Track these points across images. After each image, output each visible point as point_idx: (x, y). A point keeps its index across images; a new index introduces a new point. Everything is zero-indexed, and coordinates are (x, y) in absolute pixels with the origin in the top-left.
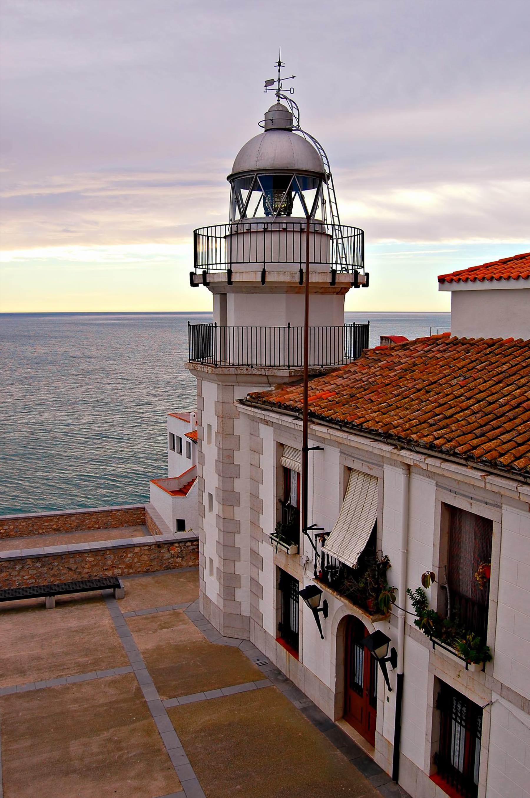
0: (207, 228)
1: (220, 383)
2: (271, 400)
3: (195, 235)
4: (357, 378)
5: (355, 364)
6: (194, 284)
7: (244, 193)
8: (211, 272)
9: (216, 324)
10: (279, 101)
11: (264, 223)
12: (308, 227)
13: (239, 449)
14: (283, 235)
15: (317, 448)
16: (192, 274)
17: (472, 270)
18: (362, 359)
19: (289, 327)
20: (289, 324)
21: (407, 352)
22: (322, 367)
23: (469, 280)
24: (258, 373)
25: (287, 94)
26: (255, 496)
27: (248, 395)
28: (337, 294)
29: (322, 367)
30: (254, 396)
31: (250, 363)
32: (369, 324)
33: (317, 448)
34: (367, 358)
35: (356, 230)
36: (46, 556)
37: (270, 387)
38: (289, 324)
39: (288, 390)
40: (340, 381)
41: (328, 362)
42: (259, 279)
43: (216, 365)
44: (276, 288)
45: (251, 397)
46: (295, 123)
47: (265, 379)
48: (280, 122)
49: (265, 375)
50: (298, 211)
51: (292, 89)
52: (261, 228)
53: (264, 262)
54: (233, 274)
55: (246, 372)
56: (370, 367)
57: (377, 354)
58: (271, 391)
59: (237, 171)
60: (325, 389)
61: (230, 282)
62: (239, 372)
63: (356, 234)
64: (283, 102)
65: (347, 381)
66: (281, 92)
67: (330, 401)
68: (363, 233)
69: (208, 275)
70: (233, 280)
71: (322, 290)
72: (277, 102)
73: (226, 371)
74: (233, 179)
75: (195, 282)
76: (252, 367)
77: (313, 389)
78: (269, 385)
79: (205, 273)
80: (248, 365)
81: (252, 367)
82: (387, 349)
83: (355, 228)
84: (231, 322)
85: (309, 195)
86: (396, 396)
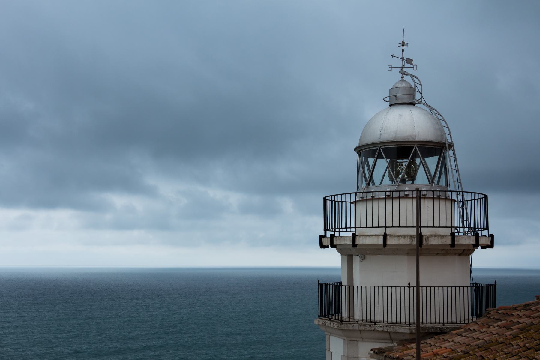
0: (335, 196)
1: (346, 338)
2: (391, 355)
4: (475, 337)
5: (476, 323)
7: (371, 161)
8: (342, 234)
9: (341, 283)
10: (403, 77)
11: (386, 192)
14: (403, 202)
16: (321, 237)
18: (484, 319)
19: (409, 287)
20: (409, 284)
21: (528, 313)
22: (444, 325)
24: (381, 329)
27: (372, 350)
28: (460, 255)
29: (444, 325)
30: (376, 351)
31: (373, 319)
32: (495, 285)
34: (489, 318)
35: (477, 195)
37: (392, 343)
38: (409, 284)
39: (408, 346)
40: (458, 339)
41: (450, 320)
42: (380, 241)
43: (342, 321)
44: (397, 251)
45: (374, 352)
46: (418, 96)
47: (387, 336)
49: (387, 332)
50: (421, 179)
51: (415, 67)
52: (382, 195)
53: (386, 227)
54: (357, 238)
55: (369, 328)
56: (489, 327)
57: (500, 313)
58: (393, 347)
59: (363, 144)
60: (442, 346)
61: (354, 245)
62: (362, 328)
63: (477, 198)
65: (465, 339)
66: (404, 70)
67: (445, 357)
69: (335, 238)
70: (357, 243)
71: (443, 252)
72: (401, 79)
73: (351, 327)
74: (359, 151)
75: (325, 244)
76: (375, 324)
77: (432, 346)
78: (391, 341)
79: (332, 236)
80: (371, 322)
81: (375, 324)
82: (511, 309)
83: (475, 193)
84: (357, 282)
85: (432, 162)
86: (506, 354)
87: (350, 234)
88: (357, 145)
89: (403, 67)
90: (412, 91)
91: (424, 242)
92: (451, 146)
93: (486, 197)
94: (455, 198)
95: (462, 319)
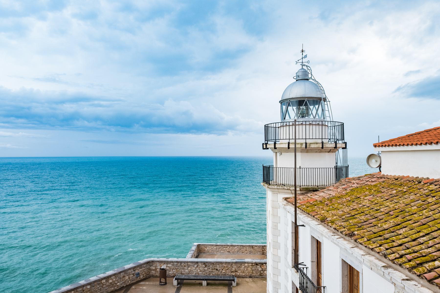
3: (266, 127)
6: (263, 149)
12: (295, 123)
13: (280, 223)
15: (303, 226)
16: (263, 144)
17: (391, 141)
23: (433, 144)
24: (287, 188)
25: (306, 64)
26: (286, 245)
28: (328, 152)
33: (303, 226)
36: (207, 262)
40: (322, 194)
42: (287, 146)
46: (310, 76)
48: (304, 77)
62: (278, 188)
64: (305, 67)
68: (343, 124)
87: (273, 143)
88: (281, 100)
89: (302, 62)
90: (305, 73)
91: (308, 146)
92: (325, 100)
93: (343, 125)
94: (326, 124)
95: (330, 183)
